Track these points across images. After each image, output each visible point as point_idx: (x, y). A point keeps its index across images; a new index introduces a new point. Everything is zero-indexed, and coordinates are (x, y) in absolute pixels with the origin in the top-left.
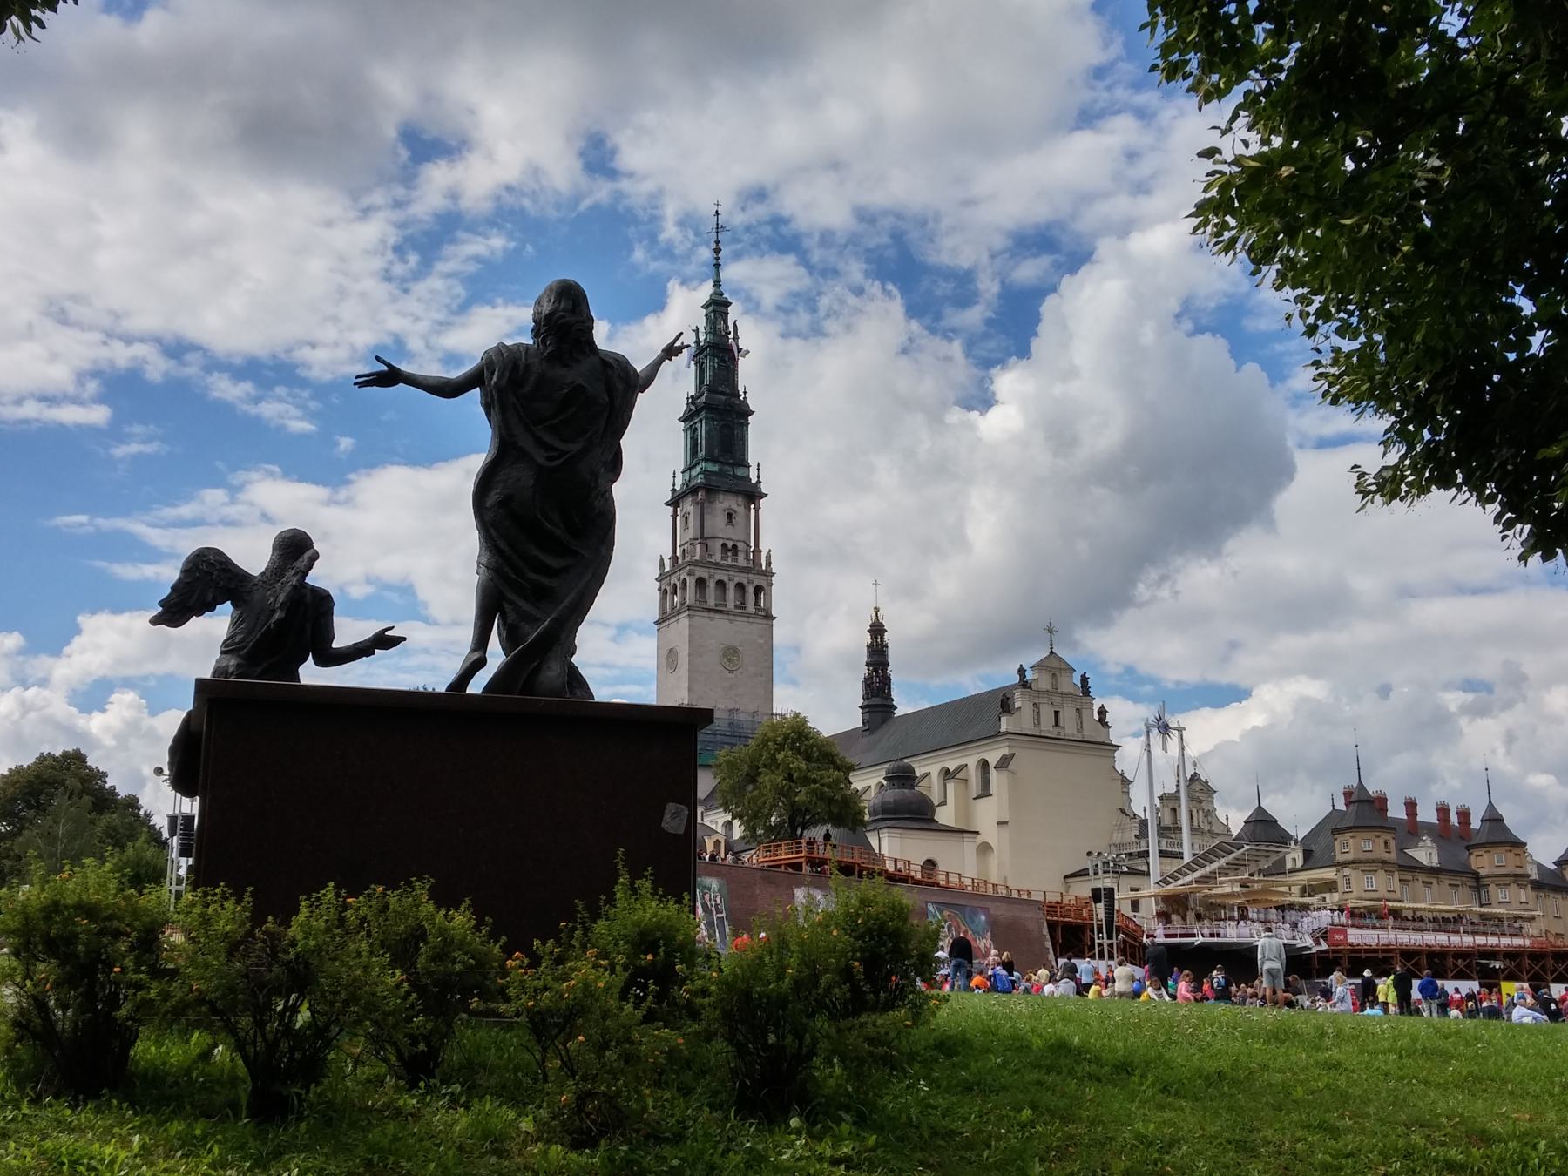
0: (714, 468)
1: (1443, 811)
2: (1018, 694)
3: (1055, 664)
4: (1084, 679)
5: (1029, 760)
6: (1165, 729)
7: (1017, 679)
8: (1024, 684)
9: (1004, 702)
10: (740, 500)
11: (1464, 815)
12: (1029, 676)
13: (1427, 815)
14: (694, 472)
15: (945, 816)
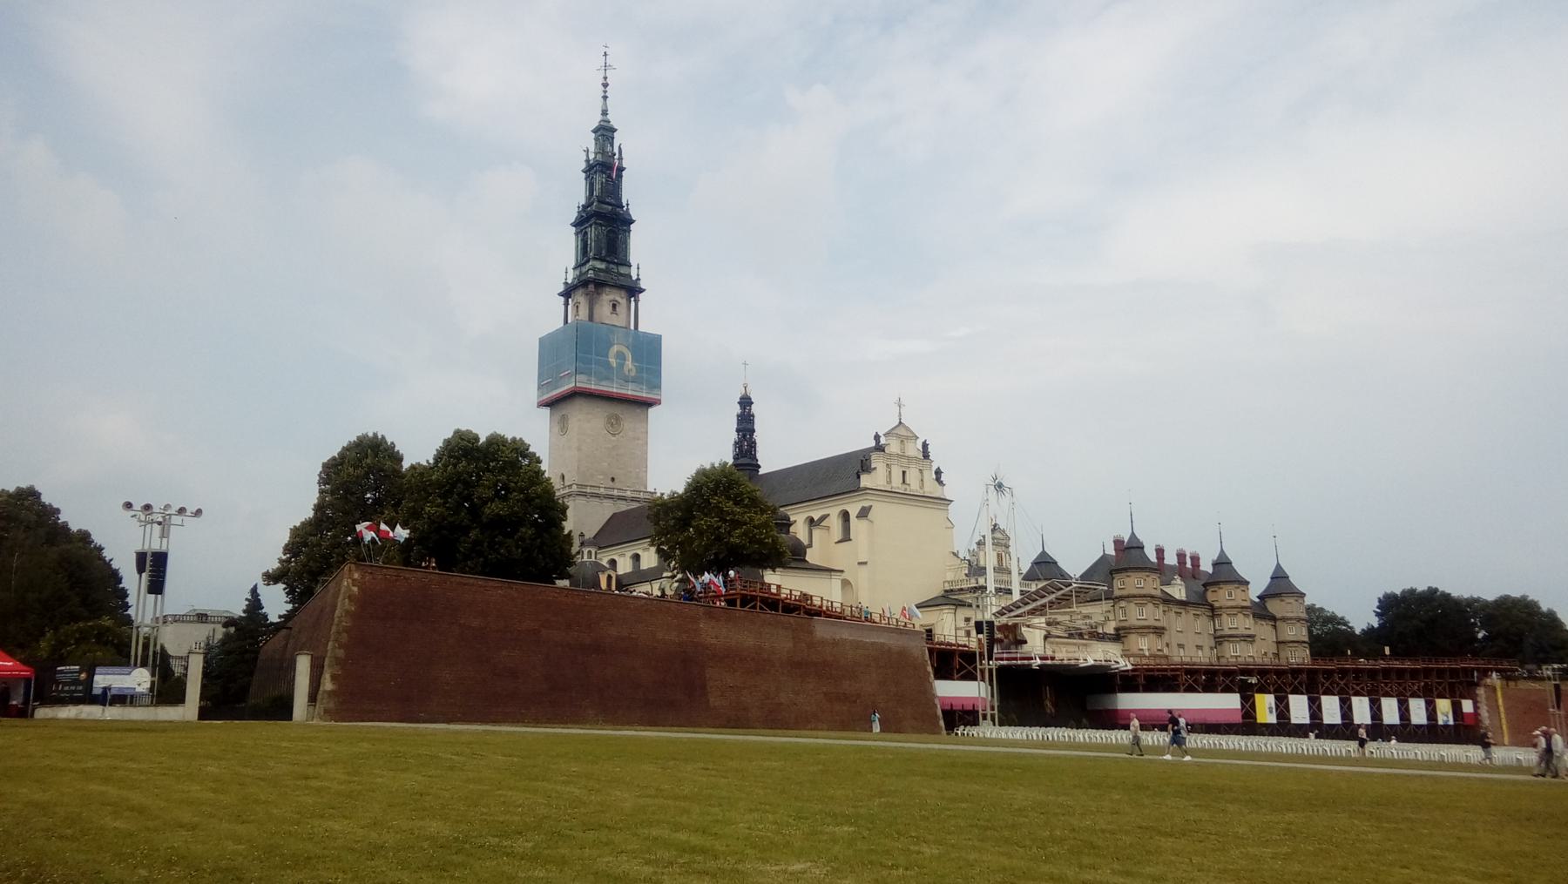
0: (602, 266)
1: (1181, 556)
2: (874, 456)
3: (902, 431)
4: (925, 445)
5: (880, 509)
6: (999, 487)
7: (873, 444)
8: (879, 448)
9: (861, 463)
10: (623, 293)
11: (1195, 560)
12: (883, 441)
13: (1171, 559)
14: (584, 269)
15: (812, 557)
